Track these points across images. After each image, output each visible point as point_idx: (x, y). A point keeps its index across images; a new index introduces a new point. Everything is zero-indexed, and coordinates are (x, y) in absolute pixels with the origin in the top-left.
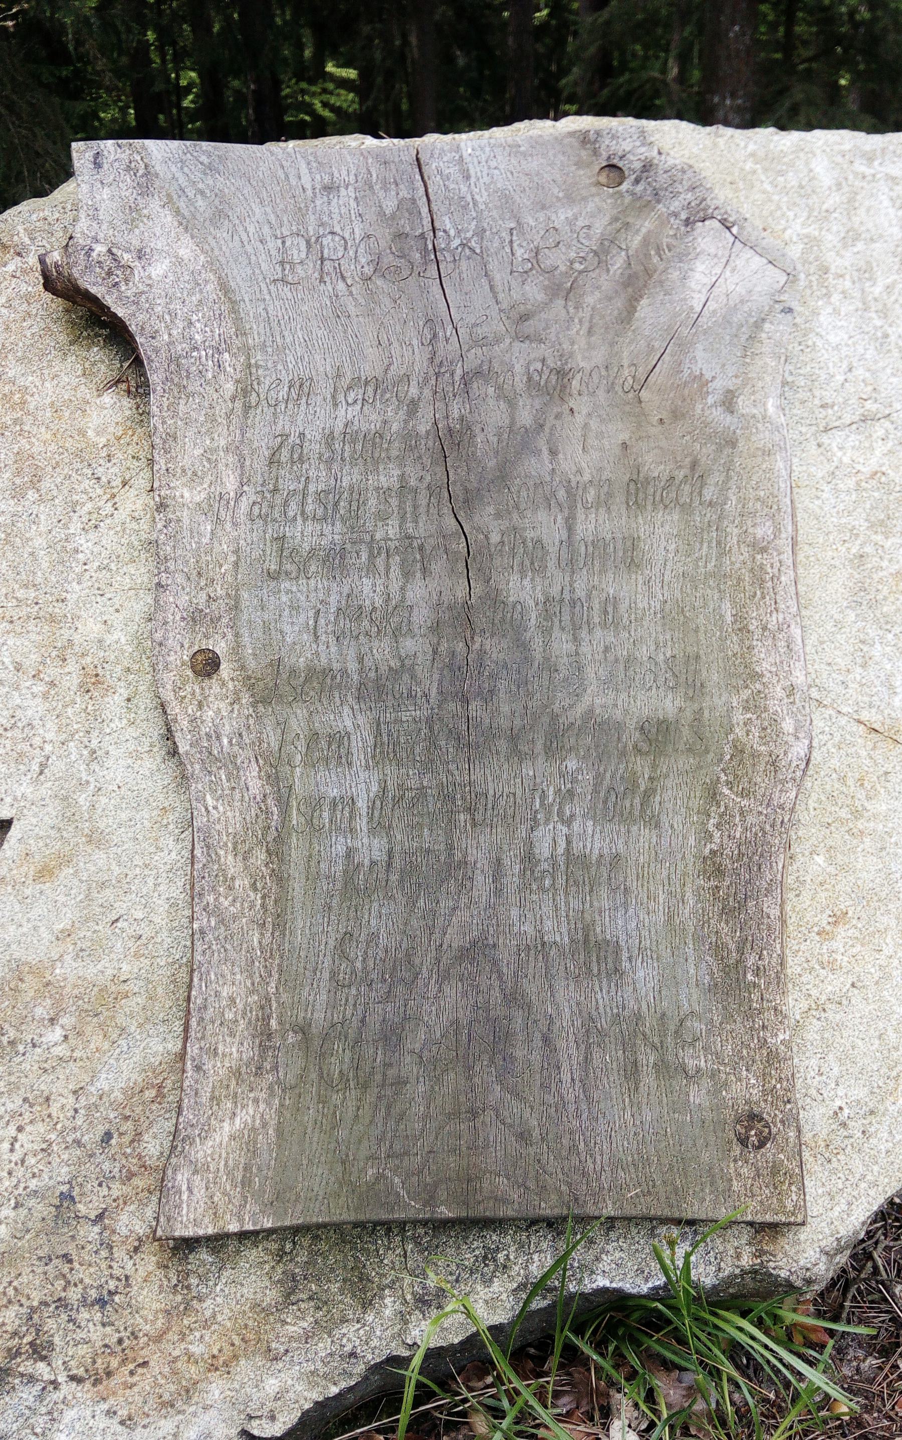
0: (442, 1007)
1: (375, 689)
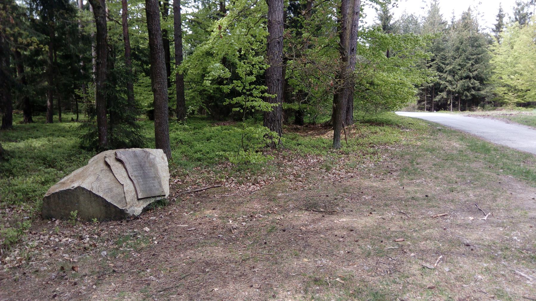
0: (148, 189)
1: (141, 176)
